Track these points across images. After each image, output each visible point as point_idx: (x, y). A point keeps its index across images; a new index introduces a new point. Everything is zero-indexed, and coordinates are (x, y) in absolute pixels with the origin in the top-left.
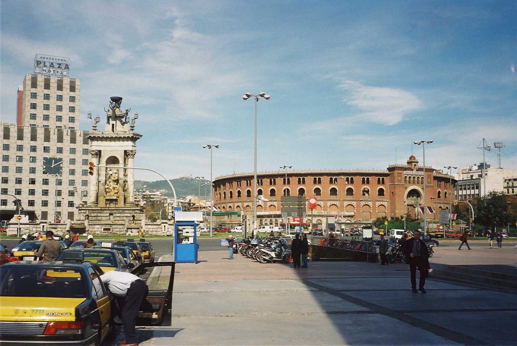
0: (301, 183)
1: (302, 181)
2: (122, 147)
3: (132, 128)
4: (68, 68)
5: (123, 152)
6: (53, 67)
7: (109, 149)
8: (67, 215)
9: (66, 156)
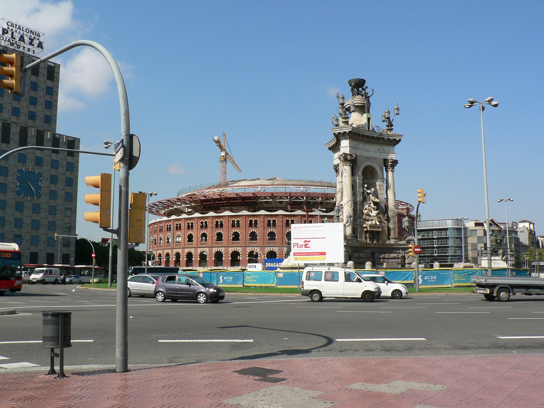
0: (219, 227)
1: (272, 224)
2: (380, 154)
3: (390, 128)
4: (42, 48)
5: (383, 162)
6: (24, 41)
7: (365, 154)
8: (29, 257)
9: (46, 170)
